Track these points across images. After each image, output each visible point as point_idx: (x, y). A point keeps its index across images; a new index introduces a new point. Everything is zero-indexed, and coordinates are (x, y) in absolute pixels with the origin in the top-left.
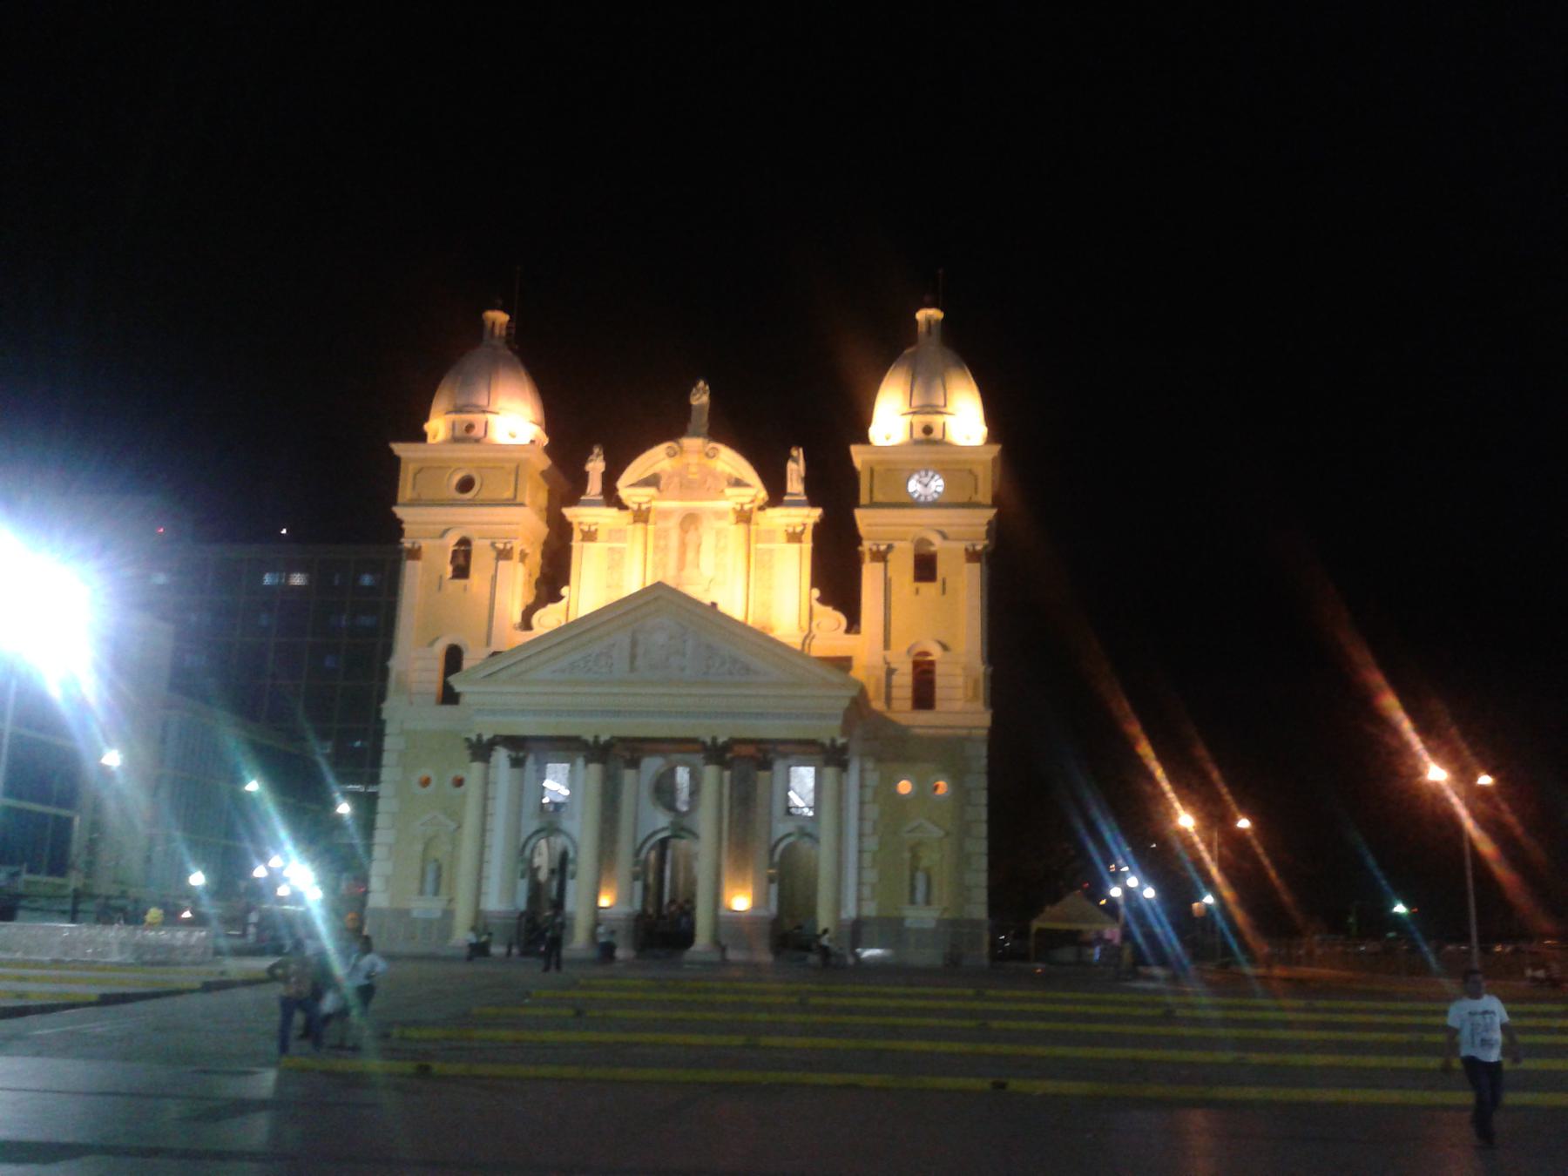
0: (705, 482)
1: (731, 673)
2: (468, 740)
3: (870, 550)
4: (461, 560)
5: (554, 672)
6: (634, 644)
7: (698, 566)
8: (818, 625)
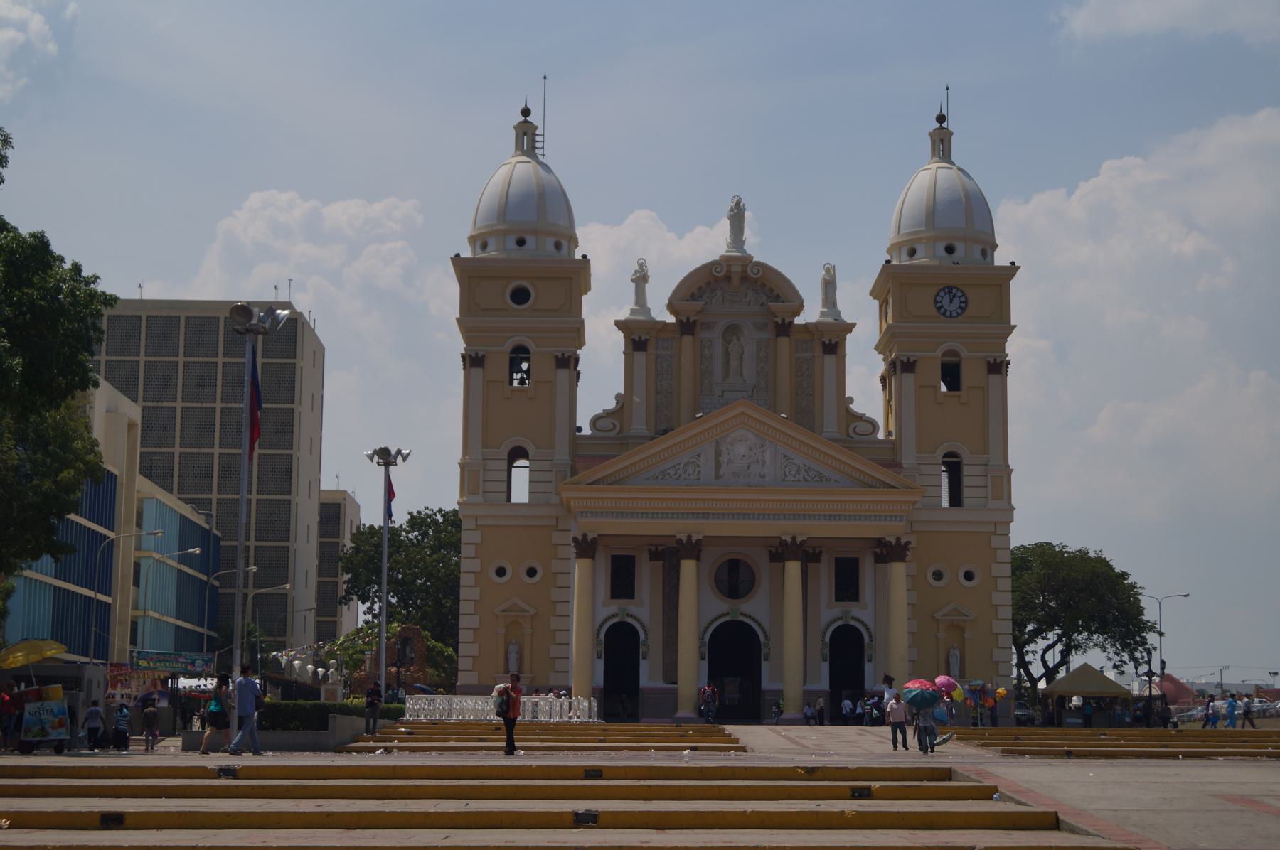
0: (747, 294)
2: (575, 539)
3: (902, 361)
5: (648, 478)
6: (718, 454)
7: (741, 375)
8: (856, 427)
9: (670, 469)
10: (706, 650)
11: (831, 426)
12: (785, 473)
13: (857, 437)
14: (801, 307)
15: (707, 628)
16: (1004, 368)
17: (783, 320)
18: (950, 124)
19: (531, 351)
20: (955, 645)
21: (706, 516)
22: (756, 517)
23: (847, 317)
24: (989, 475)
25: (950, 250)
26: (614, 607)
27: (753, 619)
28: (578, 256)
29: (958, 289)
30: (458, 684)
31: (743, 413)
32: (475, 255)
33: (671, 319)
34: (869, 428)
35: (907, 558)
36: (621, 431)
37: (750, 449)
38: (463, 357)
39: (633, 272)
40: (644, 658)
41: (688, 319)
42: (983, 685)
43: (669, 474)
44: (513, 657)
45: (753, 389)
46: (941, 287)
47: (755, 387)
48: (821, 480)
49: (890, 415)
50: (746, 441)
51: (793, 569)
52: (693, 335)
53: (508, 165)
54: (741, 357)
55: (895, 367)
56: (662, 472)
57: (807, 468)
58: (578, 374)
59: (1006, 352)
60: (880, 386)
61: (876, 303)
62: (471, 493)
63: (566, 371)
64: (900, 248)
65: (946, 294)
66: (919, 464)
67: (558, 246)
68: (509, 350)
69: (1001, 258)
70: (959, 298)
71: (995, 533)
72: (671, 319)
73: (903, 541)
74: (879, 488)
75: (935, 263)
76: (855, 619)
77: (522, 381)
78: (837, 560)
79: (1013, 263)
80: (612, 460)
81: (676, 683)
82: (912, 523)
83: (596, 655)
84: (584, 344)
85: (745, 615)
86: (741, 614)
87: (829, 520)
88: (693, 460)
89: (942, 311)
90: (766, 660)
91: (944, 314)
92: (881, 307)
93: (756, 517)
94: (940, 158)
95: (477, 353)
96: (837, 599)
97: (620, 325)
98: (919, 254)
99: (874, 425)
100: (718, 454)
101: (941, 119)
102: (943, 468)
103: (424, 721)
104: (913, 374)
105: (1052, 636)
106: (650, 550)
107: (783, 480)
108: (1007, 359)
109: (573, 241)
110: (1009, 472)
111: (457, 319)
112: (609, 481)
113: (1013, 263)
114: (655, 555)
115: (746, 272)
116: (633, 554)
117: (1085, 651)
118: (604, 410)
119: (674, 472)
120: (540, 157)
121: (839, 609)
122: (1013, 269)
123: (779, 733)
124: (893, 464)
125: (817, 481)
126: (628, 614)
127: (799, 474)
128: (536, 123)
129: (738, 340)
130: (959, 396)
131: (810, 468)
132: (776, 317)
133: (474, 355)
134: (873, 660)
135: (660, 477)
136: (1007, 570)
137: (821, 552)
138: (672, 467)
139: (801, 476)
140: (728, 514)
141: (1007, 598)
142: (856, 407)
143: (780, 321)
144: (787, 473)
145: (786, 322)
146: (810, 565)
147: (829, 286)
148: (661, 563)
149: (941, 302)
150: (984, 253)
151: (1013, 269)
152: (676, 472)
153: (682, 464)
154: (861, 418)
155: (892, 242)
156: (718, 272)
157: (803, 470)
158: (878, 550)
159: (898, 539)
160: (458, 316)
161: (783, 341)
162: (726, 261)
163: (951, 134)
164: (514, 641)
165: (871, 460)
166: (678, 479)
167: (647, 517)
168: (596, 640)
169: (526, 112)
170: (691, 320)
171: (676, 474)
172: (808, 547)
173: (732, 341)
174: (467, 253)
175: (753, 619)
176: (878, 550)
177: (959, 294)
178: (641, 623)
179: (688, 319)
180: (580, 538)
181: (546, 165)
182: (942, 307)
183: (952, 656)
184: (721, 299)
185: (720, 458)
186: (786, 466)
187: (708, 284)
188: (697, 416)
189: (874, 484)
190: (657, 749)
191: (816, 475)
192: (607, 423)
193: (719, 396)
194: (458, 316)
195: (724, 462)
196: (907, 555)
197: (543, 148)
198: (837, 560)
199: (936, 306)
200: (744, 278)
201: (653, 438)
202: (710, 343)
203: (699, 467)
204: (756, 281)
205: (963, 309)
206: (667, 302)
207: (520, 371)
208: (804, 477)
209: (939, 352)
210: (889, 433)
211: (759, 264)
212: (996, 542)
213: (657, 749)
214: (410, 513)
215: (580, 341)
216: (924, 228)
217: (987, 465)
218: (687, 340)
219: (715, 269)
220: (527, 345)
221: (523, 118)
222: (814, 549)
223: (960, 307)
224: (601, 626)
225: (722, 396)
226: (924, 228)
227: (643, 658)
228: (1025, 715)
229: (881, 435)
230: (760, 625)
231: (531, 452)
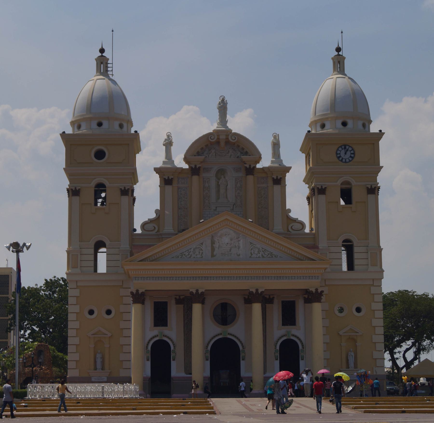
0: (229, 151)
2: (132, 293)
3: (318, 188)
5: (173, 257)
6: (213, 243)
7: (227, 197)
8: (292, 227)
9: (185, 252)
10: (208, 355)
11: (278, 226)
13: (293, 232)
14: (260, 158)
15: (209, 342)
16: (376, 191)
18: (343, 53)
19: (107, 186)
20: (352, 350)
21: (206, 278)
22: (235, 278)
23: (286, 164)
24: (369, 252)
25: (344, 124)
26: (156, 331)
27: (235, 337)
28: (133, 131)
29: (350, 146)
30: (68, 376)
31: (227, 219)
32: (74, 132)
33: (186, 166)
34: (300, 226)
35: (322, 301)
36: (158, 231)
38: (68, 190)
39: (164, 140)
40: (174, 360)
41: (196, 166)
42: (365, 372)
43: (185, 255)
44: (99, 361)
45: (234, 206)
46: (340, 145)
47: (234, 204)
48: (272, 257)
49: (312, 219)
50: (229, 235)
51: (257, 308)
52: (199, 175)
53: (92, 81)
54: (226, 187)
55: (314, 191)
56: (181, 253)
57: (264, 250)
58: (134, 199)
59: (378, 182)
60: (306, 202)
61: (304, 155)
62: (73, 268)
63: (128, 196)
64: (316, 123)
65: (342, 149)
66: (328, 246)
67: (121, 126)
68: (94, 186)
69: (374, 129)
70: (350, 151)
71: (373, 285)
72: (186, 166)
73: (319, 291)
74: (305, 260)
75: (337, 131)
76: (293, 335)
77: (102, 204)
78: (283, 302)
79: (380, 131)
80: (153, 247)
81: (191, 374)
82: (325, 280)
83: (146, 359)
84: (138, 182)
85: (231, 334)
86: (229, 334)
87: (277, 279)
88: (199, 246)
89: (340, 159)
90: (243, 360)
91: (342, 161)
92: (306, 157)
93: (235, 278)
94: (338, 72)
95: (75, 188)
96: (283, 325)
97: (157, 170)
98: (326, 128)
99: (302, 224)
100: (213, 243)
101: (338, 49)
102: (343, 249)
103: (39, 399)
104: (325, 195)
105: (409, 343)
106: (176, 298)
107: (250, 257)
108: (378, 185)
109: (130, 123)
110: (381, 250)
111: (64, 169)
112: (151, 259)
113: (380, 131)
114: (179, 301)
115: (228, 139)
116: (166, 301)
117: (428, 352)
118: (148, 219)
119: (188, 253)
120: (111, 76)
121: (284, 330)
122: (381, 134)
123: (240, 402)
124: (314, 247)
125: (270, 257)
126: (164, 335)
127: (259, 253)
128: (108, 57)
129: (224, 177)
130: (351, 207)
131: (265, 250)
132: (246, 164)
133: (74, 189)
134: (304, 359)
135: (180, 256)
136: (380, 306)
137: (273, 298)
138: (187, 250)
139: (261, 254)
140: (219, 277)
141: (381, 322)
142: (292, 215)
143: (248, 166)
144: (253, 253)
145: (252, 167)
146: (267, 305)
147: (276, 146)
148: (183, 305)
149: (340, 154)
150: (364, 125)
151: (381, 134)
152: (189, 253)
153: (192, 249)
154: (295, 221)
155: (312, 120)
156: (212, 139)
157: (261, 251)
158: (306, 296)
159: (317, 290)
160: (65, 167)
162: (216, 132)
163: (344, 58)
164: (99, 351)
165: (300, 244)
166: (190, 257)
167: (173, 280)
168: (146, 351)
169: (102, 51)
170: (197, 167)
171: (189, 254)
172: (266, 295)
174: (69, 130)
175: (235, 337)
176: (306, 296)
177: (350, 149)
178: (172, 340)
179: (196, 166)
180: (135, 292)
181: (114, 81)
182: (340, 157)
183: (349, 356)
184: (214, 154)
185: (214, 245)
187: (207, 146)
188: (201, 221)
189: (302, 258)
190: (164, 413)
191: (269, 254)
192: (150, 227)
193: (214, 210)
194: (65, 167)
195: (216, 248)
196: (322, 299)
197: (112, 71)
198: (283, 302)
199: (337, 156)
200: (227, 142)
201: (177, 234)
202: (208, 179)
204: (234, 144)
205: (353, 158)
206: (184, 157)
207: (101, 198)
209: (339, 182)
210: (312, 229)
211: (235, 134)
212: (374, 290)
213: (164, 413)
214: (46, 280)
215: (135, 180)
216: (329, 112)
217: (368, 246)
218: (195, 178)
219: (211, 137)
220: (105, 183)
221: (100, 54)
222: (270, 296)
223: (351, 157)
224: (148, 342)
225: (216, 210)
226: (329, 112)
228: (393, 389)
229: (307, 230)
230: (239, 340)
231: (107, 243)
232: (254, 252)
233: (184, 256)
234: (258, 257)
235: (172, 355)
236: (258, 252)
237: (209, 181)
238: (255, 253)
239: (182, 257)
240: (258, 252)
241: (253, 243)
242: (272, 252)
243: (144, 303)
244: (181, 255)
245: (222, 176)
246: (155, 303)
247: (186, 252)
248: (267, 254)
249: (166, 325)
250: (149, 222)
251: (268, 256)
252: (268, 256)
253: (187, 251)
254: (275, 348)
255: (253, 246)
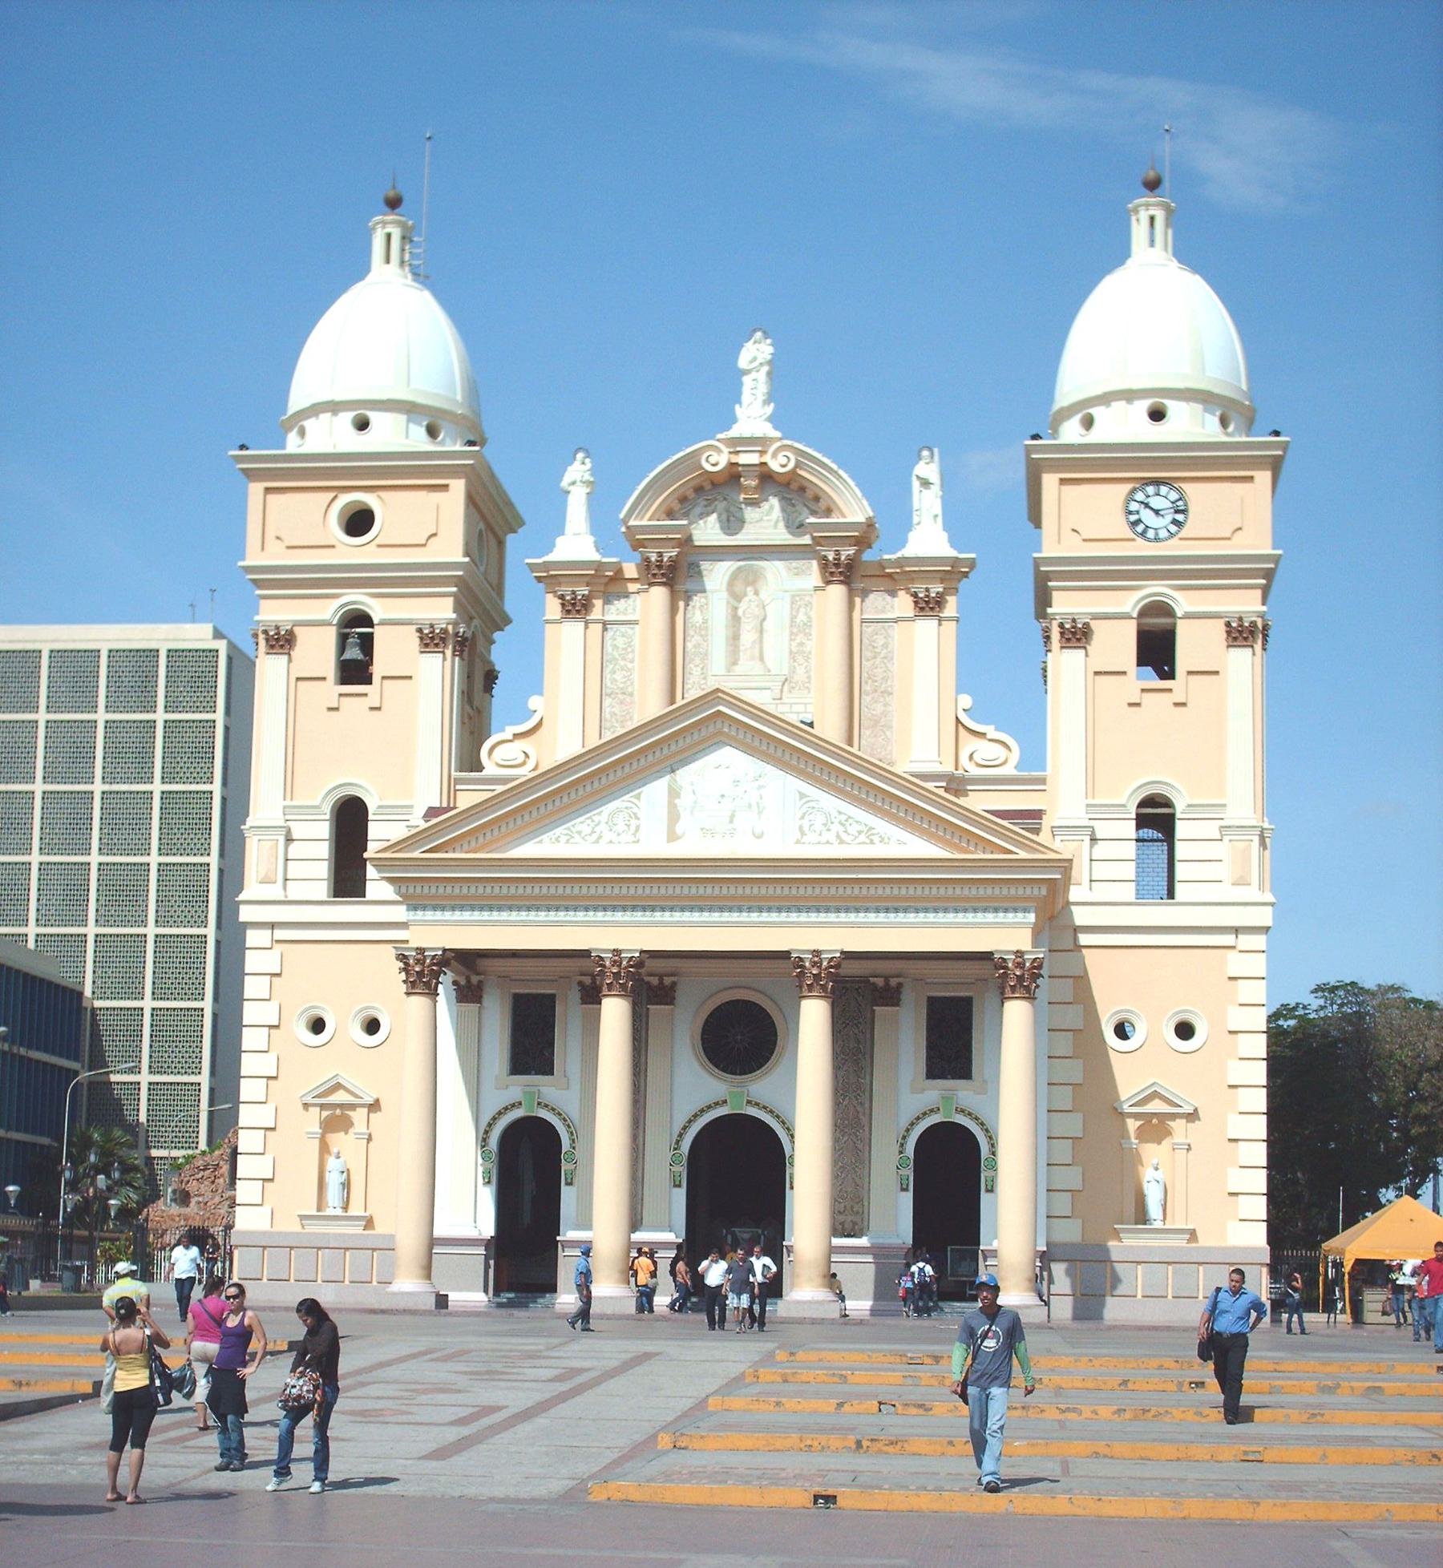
1: (842, 842)
4: (354, 653)
6: (673, 793)
7: (761, 659)
12: (801, 828)
17: (838, 553)
19: (376, 621)
26: (517, 1088)
37: (736, 782)
43: (579, 833)
47: (786, 680)
48: (872, 842)
57: (843, 818)
68: (335, 622)
78: (932, 1002)
86: (749, 1102)
88: (630, 805)
91: (1143, 534)
100: (673, 793)
106: (580, 983)
121: (934, 1092)
125: (864, 843)
126: (539, 1104)
127: (829, 830)
129: (756, 593)
131: (850, 817)
137: (900, 985)
144: (806, 829)
156: (713, 465)
157: (836, 821)
161: (837, 591)
166: (597, 841)
171: (593, 832)
173: (745, 595)
177: (1174, 496)
182: (1139, 521)
185: (677, 801)
186: (804, 814)
187: (699, 490)
191: (860, 832)
198: (932, 1002)
203: (638, 819)
208: (838, 836)
218: (659, 594)
223: (1175, 522)
227: (567, 1184)
232: (811, 826)
233: (576, 836)
234: (823, 839)
235: (565, 1167)
236: (825, 825)
237: (707, 604)
238: (812, 828)
239: (572, 841)
240: (825, 825)
241: (807, 796)
242: (871, 824)
243: (481, 997)
244: (566, 835)
245: (749, 589)
246: (517, 998)
247: (585, 824)
248: (857, 834)
249: (550, 1071)
250: (511, 737)
251: (858, 841)
252: (858, 841)
253: (589, 821)
254: (901, 1152)
255: (805, 806)
